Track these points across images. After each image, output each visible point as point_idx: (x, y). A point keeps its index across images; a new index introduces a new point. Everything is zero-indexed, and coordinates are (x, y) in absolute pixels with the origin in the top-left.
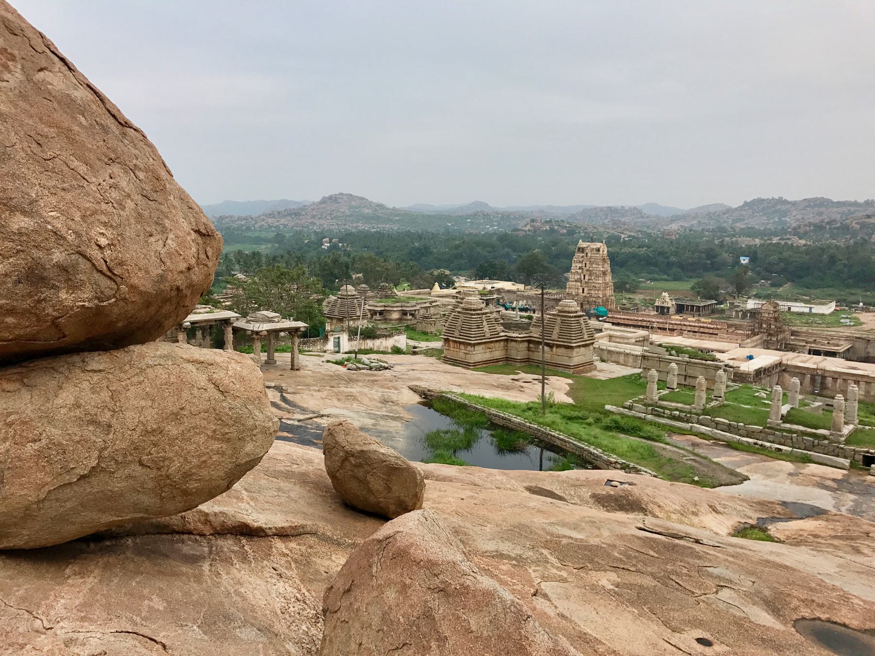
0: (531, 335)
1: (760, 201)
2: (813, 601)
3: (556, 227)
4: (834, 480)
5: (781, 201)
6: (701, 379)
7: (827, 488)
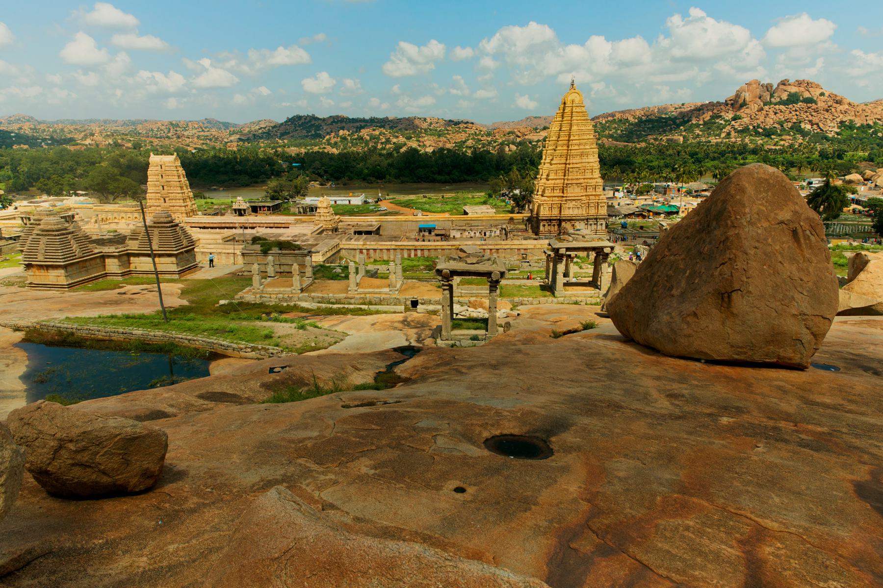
0: (128, 248)
1: (299, 118)
2: (487, 423)
3: (119, 141)
4: (399, 322)
5: (314, 118)
6: (296, 267)
7: (395, 328)
